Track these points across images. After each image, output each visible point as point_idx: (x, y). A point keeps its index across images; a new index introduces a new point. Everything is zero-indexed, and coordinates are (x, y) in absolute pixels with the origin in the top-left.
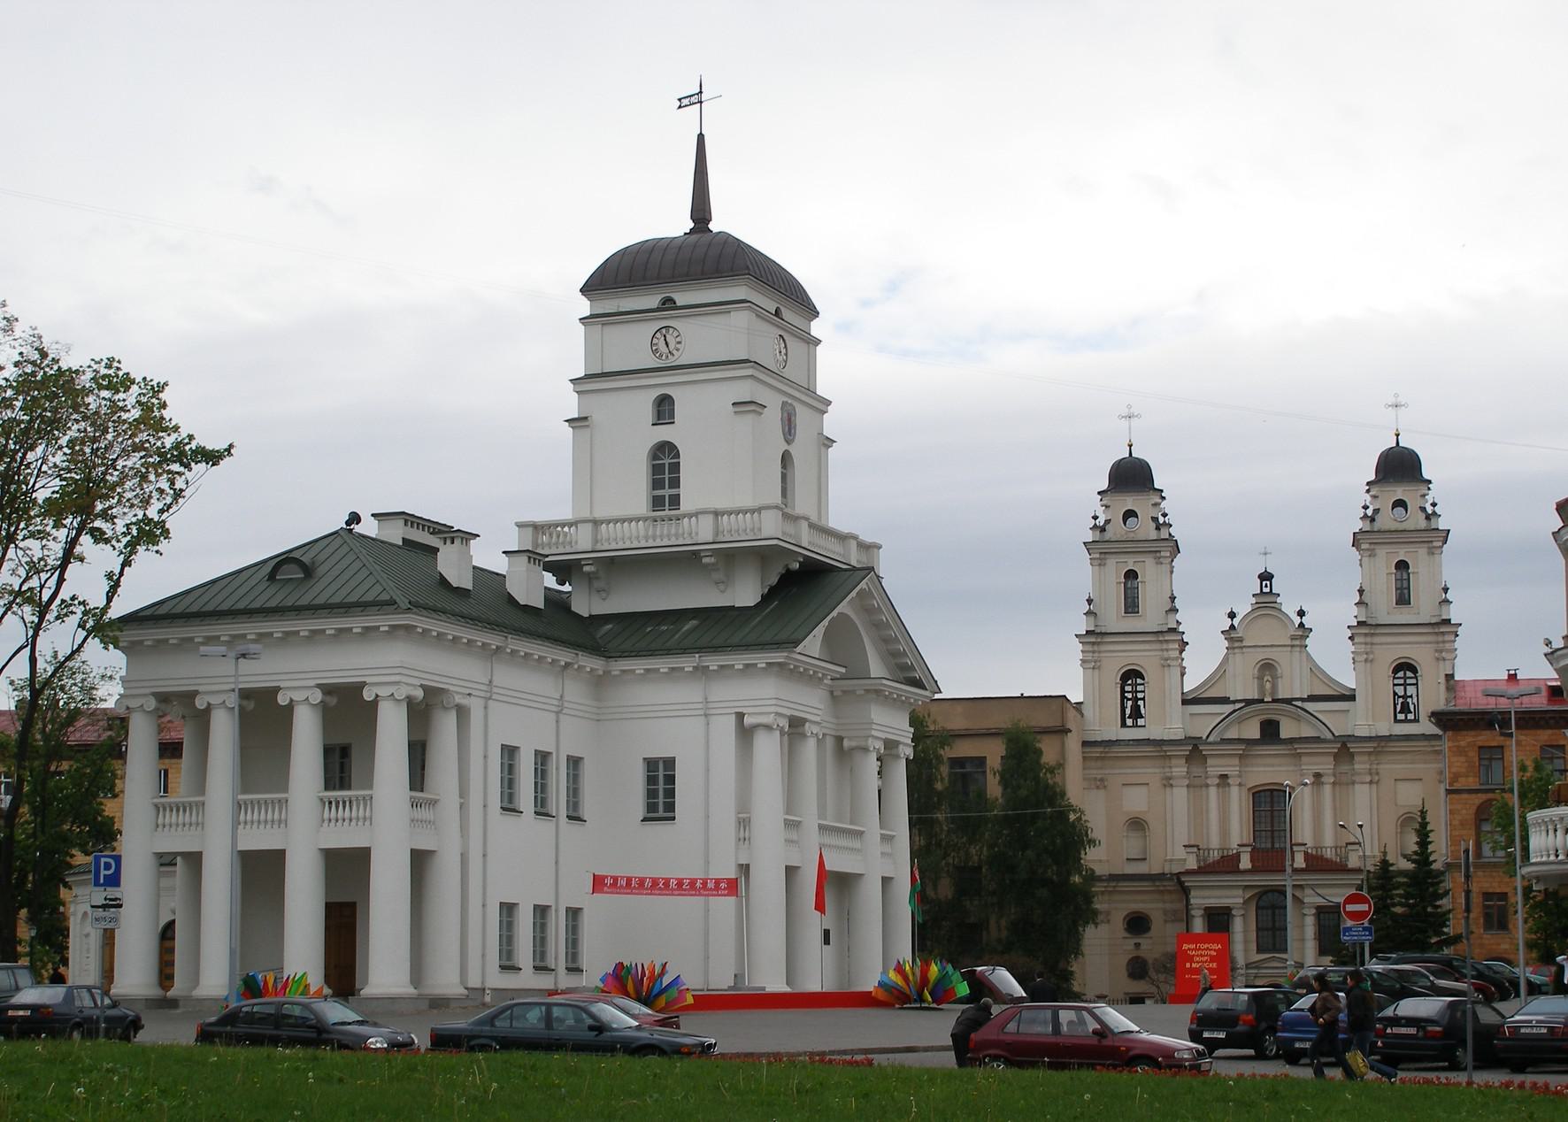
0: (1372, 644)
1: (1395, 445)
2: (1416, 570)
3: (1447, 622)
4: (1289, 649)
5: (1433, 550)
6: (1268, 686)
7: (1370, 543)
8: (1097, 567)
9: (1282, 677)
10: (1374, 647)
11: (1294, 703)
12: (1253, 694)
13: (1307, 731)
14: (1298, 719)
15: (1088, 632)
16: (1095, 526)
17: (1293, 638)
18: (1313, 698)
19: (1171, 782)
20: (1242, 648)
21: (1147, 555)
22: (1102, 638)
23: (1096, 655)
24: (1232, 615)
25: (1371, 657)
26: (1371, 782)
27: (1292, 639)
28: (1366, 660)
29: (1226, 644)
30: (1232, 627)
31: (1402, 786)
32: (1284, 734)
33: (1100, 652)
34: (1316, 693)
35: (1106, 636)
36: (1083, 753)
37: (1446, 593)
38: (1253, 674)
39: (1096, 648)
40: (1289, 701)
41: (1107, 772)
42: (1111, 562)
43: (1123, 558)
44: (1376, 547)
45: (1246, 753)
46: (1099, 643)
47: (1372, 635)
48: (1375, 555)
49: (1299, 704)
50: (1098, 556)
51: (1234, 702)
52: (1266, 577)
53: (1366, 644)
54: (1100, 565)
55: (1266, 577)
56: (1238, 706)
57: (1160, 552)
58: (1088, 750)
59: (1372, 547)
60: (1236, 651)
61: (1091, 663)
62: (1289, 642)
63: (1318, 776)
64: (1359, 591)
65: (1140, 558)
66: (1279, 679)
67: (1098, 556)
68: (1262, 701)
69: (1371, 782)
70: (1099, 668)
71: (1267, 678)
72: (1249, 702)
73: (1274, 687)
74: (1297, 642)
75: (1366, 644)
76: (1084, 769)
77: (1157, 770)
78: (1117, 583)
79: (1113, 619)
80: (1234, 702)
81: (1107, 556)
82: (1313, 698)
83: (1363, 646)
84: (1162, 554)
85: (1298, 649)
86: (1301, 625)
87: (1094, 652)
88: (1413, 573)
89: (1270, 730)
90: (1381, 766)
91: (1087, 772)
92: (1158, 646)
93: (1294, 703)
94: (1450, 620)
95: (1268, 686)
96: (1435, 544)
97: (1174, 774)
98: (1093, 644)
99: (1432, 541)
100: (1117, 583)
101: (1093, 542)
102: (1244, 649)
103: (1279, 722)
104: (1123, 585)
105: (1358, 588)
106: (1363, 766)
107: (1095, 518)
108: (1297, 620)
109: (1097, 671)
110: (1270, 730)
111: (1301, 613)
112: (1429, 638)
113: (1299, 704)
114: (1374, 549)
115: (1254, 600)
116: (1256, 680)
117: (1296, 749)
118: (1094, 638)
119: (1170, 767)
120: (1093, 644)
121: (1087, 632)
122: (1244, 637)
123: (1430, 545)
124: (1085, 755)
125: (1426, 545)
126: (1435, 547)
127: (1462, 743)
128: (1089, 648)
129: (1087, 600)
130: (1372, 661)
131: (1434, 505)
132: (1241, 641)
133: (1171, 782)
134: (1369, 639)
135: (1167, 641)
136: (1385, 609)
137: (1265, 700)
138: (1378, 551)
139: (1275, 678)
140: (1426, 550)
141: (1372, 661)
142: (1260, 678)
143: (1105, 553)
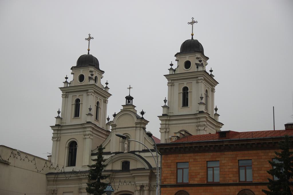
0: (169, 124)
1: (191, 39)
2: (191, 91)
4: (135, 129)
5: (198, 81)
6: (126, 146)
7: (172, 80)
8: (65, 98)
10: (169, 126)
11: (136, 153)
13: (140, 166)
14: (136, 160)
15: (56, 125)
16: (66, 82)
17: (136, 124)
18: (144, 151)
19: (81, 191)
22: (61, 128)
23: (59, 135)
25: (168, 130)
27: (136, 124)
28: (165, 132)
32: (131, 167)
33: (60, 134)
35: (63, 127)
36: (47, 178)
38: (120, 141)
39: (59, 132)
40: (133, 152)
41: (58, 187)
42: (70, 96)
45: (113, 177)
46: (60, 130)
47: (169, 120)
48: (174, 85)
49: (137, 153)
50: (65, 93)
51: (111, 154)
52: (129, 99)
55: (129, 99)
56: (112, 155)
57: (88, 90)
58: (48, 176)
59: (173, 82)
61: (56, 139)
62: (135, 125)
63: (142, 187)
67: (65, 93)
68: (123, 153)
70: (60, 140)
72: (116, 153)
74: (139, 126)
75: (166, 124)
76: (48, 185)
77: (77, 185)
79: (69, 120)
81: (69, 94)
82: (144, 151)
83: (164, 125)
84: (89, 91)
85: (139, 129)
86: (142, 118)
87: (57, 134)
88: (190, 92)
89: (126, 166)
91: (49, 187)
93: (136, 153)
96: (199, 78)
97: (83, 187)
98: (58, 130)
100: (72, 105)
101: (64, 87)
102: (117, 130)
103: (129, 162)
105: (164, 99)
107: (67, 78)
108: (141, 116)
109: (58, 142)
110: (126, 166)
111: (143, 113)
113: (137, 153)
114: (173, 83)
115: (122, 108)
116: (121, 143)
117: (131, 174)
118: (58, 128)
119: (81, 184)
120: (58, 130)
121: (56, 125)
122: (116, 124)
124: (48, 179)
126: (199, 80)
127: (169, 161)
128: (56, 132)
129: (58, 112)
130: (168, 132)
132: (116, 126)
133: (81, 191)
134: (167, 123)
135: (86, 128)
136: (177, 109)
137: (125, 152)
138: (175, 84)
140: (196, 81)
141: (168, 132)
143: (68, 92)
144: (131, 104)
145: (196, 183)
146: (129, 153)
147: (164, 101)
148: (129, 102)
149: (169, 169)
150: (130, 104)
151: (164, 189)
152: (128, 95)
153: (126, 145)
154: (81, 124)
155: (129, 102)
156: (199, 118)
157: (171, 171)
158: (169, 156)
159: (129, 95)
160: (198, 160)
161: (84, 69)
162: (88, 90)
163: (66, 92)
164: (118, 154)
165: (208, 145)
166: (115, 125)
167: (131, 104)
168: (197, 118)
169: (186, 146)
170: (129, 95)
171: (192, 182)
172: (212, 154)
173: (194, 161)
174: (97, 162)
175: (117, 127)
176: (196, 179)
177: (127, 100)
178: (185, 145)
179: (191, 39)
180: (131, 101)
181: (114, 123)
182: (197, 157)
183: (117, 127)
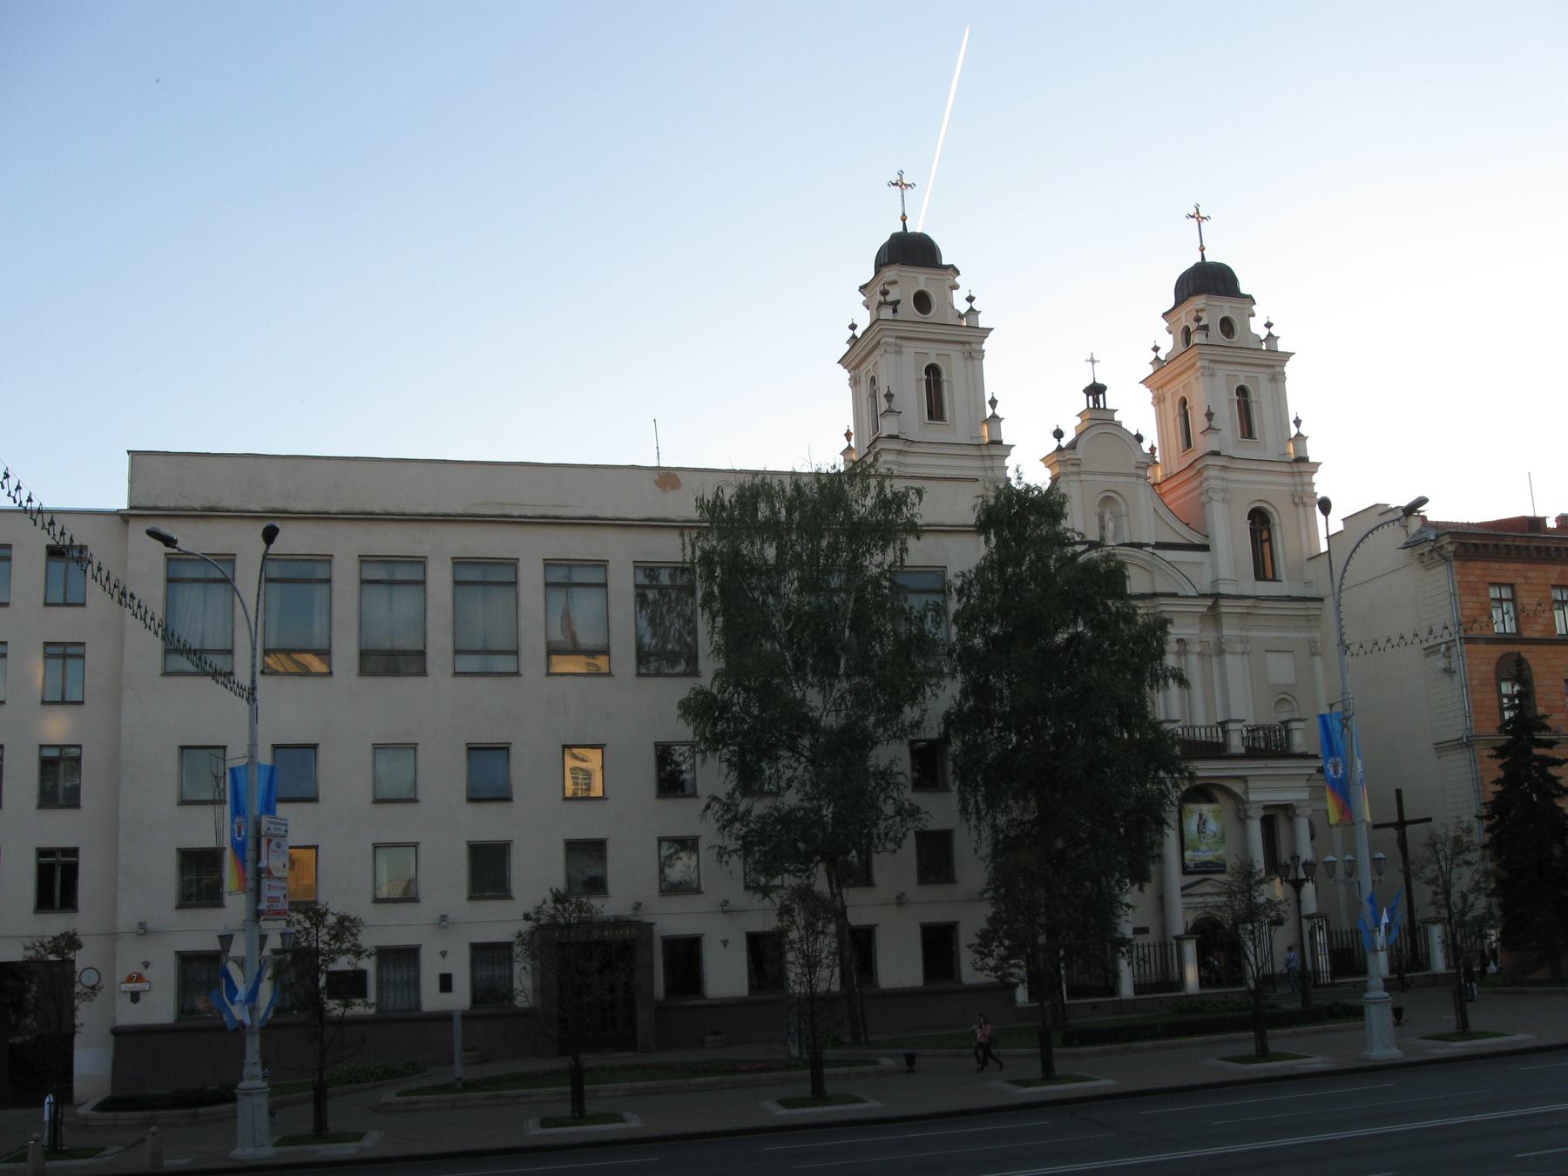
3: (1303, 460)
4: (1134, 480)
7: (1211, 361)
9: (1127, 515)
20: (1078, 474)
21: (952, 347)
22: (909, 447)
24: (1058, 434)
26: (1243, 653)
30: (1059, 449)
31: (1273, 659)
35: (917, 444)
40: (1140, 546)
44: (1217, 366)
52: (1095, 390)
53: (1223, 479)
55: (1095, 390)
59: (1212, 365)
60: (1071, 478)
62: (1133, 471)
64: (1206, 415)
65: (943, 349)
66: (1125, 519)
69: (1243, 653)
73: (1117, 530)
74: (1141, 472)
75: (1223, 479)
78: (917, 380)
81: (905, 343)
90: (1250, 634)
94: (1308, 458)
95: (1110, 526)
99: (1273, 366)
102: (1083, 477)
106: (1232, 632)
112: (1288, 480)
123: (1272, 370)
125: (1266, 370)
127: (1473, 578)
131: (1269, 325)
139: (1117, 517)
144: (1102, 406)
145: (1537, 635)
147: (1206, 415)
148: (1096, 401)
149: (1474, 597)
150: (1099, 405)
151: (1473, 647)
152: (1092, 382)
155: (1096, 401)
157: (1481, 602)
158: (1471, 564)
159: (1094, 382)
160: (1535, 581)
161: (928, 276)
162: (970, 343)
163: (897, 337)
165: (1562, 546)
166: (1074, 462)
168: (1292, 474)
169: (1517, 543)
170: (1094, 382)
171: (1527, 634)
172: (1559, 568)
173: (1526, 584)
174: (771, 562)
175: (1083, 468)
176: (1537, 627)
177: (1091, 398)
178: (1514, 541)
179: (1200, 260)
180: (1101, 396)
182: (1532, 574)
183: (1083, 468)
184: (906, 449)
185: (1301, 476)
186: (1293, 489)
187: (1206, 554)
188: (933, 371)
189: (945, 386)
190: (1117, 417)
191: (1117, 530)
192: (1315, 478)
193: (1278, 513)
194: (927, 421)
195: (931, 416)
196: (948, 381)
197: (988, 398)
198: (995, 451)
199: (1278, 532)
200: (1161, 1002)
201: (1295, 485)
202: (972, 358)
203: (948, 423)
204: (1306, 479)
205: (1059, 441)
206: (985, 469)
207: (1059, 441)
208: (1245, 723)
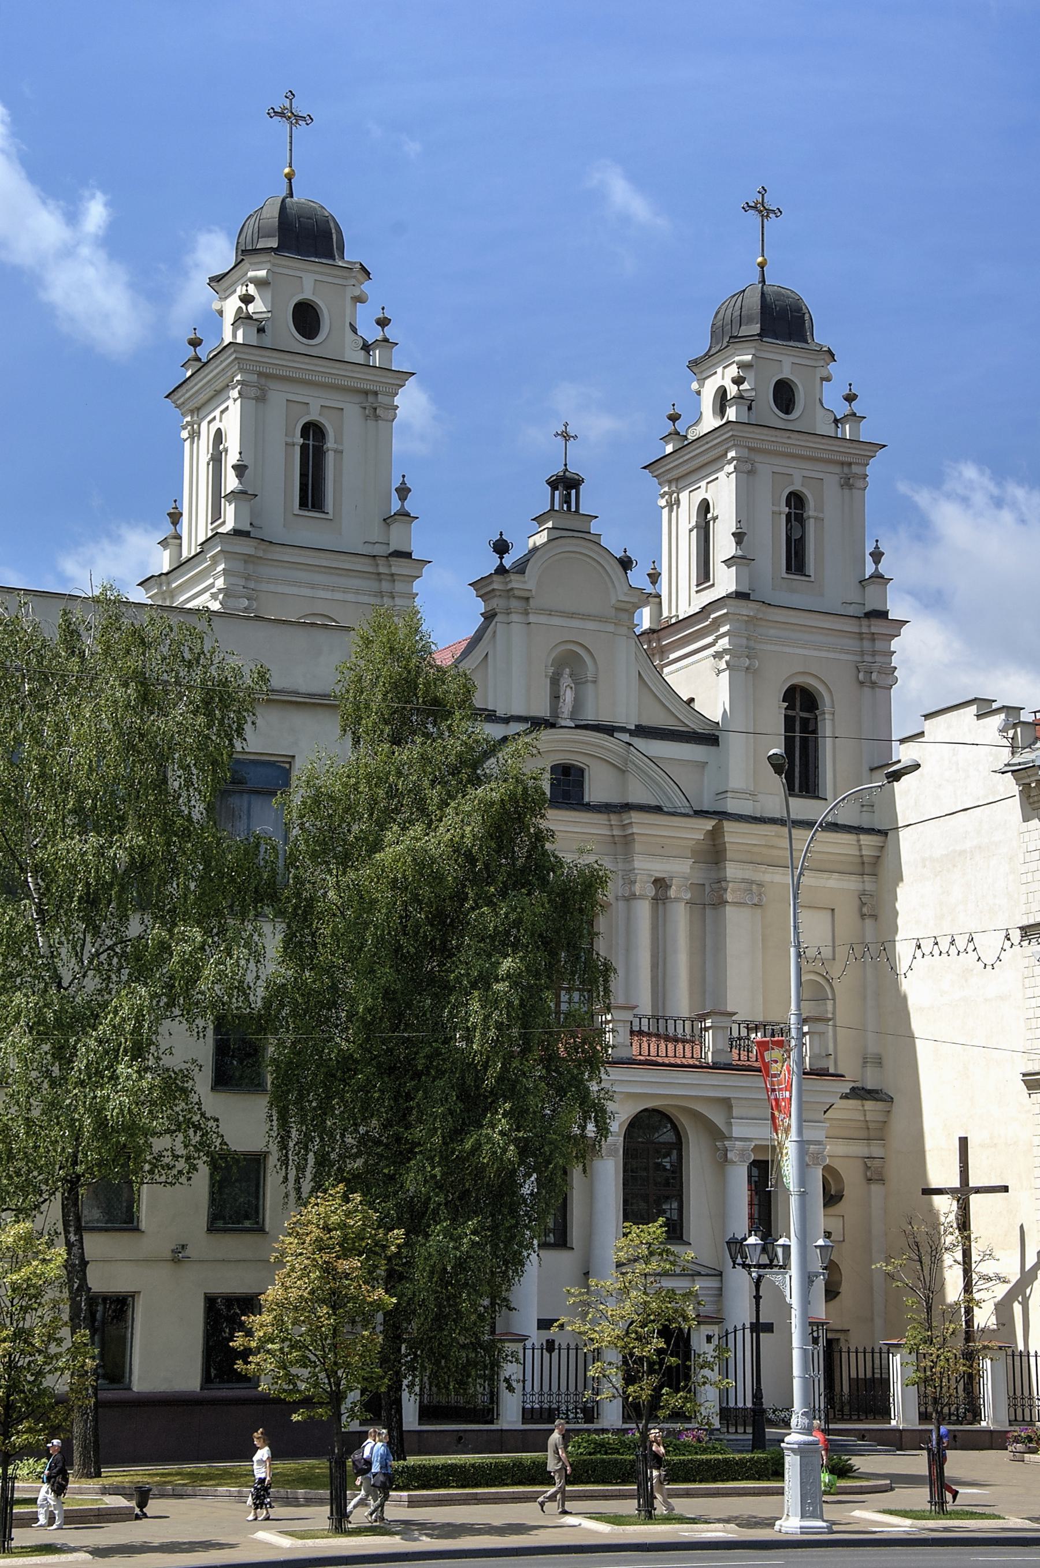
9: (595, 682)
11: (616, 735)
12: (541, 709)
18: (643, 731)
24: (501, 547)
29: (481, 606)
30: (501, 570)
34: (645, 722)
37: (877, 562)
40: (609, 730)
42: (278, 396)
43: (301, 394)
44: (758, 458)
50: (254, 378)
51: (507, 720)
54: (257, 399)
63: (661, 884)
65: (334, 400)
66: (590, 685)
71: (566, 681)
73: (578, 704)
80: (507, 720)
82: (643, 731)
92: (372, 585)
94: (886, 613)
98: (248, 559)
103: (581, 771)
104: (297, 450)
132: (527, 599)
139: (579, 683)
142: (555, 682)
144: (573, 509)
146: (577, 727)
150: (569, 508)
153: (568, 690)
154: (374, 556)
156: (873, 638)
163: (260, 374)
164: (602, 735)
166: (526, 594)
167: (573, 509)
180: (573, 492)
181: (525, 582)
184: (261, 554)
185: (873, 640)
186: (858, 658)
187: (713, 749)
188: (313, 431)
189: (330, 459)
190: (594, 527)
191: (578, 704)
192: (895, 644)
193: (830, 692)
194: (297, 511)
195: (303, 504)
196: (335, 451)
197: (396, 483)
198: (399, 567)
199: (828, 723)
200: (461, 1438)
201: (862, 653)
202: (377, 418)
203: (330, 517)
204: (879, 645)
205: (501, 558)
206: (380, 594)
207: (501, 558)
208: (635, 1012)
